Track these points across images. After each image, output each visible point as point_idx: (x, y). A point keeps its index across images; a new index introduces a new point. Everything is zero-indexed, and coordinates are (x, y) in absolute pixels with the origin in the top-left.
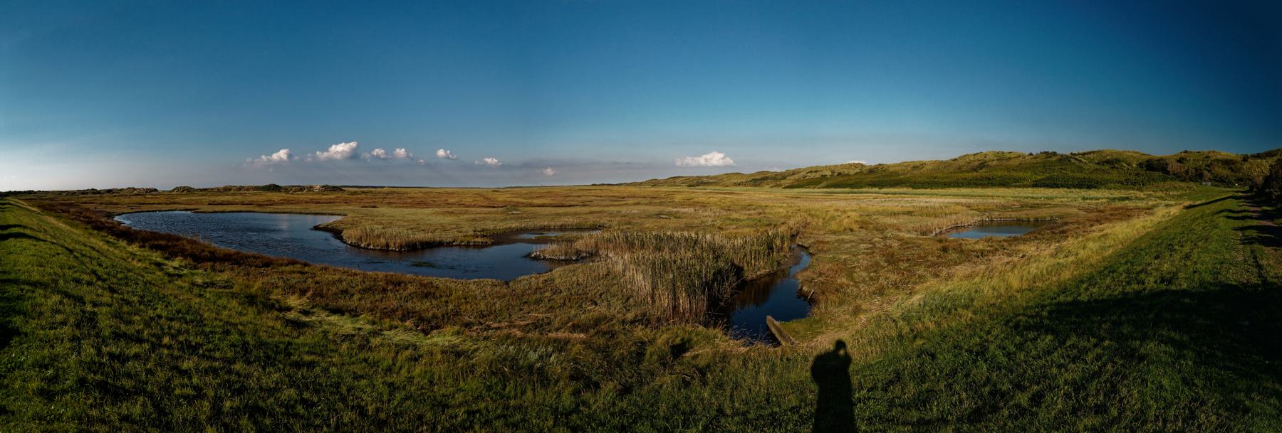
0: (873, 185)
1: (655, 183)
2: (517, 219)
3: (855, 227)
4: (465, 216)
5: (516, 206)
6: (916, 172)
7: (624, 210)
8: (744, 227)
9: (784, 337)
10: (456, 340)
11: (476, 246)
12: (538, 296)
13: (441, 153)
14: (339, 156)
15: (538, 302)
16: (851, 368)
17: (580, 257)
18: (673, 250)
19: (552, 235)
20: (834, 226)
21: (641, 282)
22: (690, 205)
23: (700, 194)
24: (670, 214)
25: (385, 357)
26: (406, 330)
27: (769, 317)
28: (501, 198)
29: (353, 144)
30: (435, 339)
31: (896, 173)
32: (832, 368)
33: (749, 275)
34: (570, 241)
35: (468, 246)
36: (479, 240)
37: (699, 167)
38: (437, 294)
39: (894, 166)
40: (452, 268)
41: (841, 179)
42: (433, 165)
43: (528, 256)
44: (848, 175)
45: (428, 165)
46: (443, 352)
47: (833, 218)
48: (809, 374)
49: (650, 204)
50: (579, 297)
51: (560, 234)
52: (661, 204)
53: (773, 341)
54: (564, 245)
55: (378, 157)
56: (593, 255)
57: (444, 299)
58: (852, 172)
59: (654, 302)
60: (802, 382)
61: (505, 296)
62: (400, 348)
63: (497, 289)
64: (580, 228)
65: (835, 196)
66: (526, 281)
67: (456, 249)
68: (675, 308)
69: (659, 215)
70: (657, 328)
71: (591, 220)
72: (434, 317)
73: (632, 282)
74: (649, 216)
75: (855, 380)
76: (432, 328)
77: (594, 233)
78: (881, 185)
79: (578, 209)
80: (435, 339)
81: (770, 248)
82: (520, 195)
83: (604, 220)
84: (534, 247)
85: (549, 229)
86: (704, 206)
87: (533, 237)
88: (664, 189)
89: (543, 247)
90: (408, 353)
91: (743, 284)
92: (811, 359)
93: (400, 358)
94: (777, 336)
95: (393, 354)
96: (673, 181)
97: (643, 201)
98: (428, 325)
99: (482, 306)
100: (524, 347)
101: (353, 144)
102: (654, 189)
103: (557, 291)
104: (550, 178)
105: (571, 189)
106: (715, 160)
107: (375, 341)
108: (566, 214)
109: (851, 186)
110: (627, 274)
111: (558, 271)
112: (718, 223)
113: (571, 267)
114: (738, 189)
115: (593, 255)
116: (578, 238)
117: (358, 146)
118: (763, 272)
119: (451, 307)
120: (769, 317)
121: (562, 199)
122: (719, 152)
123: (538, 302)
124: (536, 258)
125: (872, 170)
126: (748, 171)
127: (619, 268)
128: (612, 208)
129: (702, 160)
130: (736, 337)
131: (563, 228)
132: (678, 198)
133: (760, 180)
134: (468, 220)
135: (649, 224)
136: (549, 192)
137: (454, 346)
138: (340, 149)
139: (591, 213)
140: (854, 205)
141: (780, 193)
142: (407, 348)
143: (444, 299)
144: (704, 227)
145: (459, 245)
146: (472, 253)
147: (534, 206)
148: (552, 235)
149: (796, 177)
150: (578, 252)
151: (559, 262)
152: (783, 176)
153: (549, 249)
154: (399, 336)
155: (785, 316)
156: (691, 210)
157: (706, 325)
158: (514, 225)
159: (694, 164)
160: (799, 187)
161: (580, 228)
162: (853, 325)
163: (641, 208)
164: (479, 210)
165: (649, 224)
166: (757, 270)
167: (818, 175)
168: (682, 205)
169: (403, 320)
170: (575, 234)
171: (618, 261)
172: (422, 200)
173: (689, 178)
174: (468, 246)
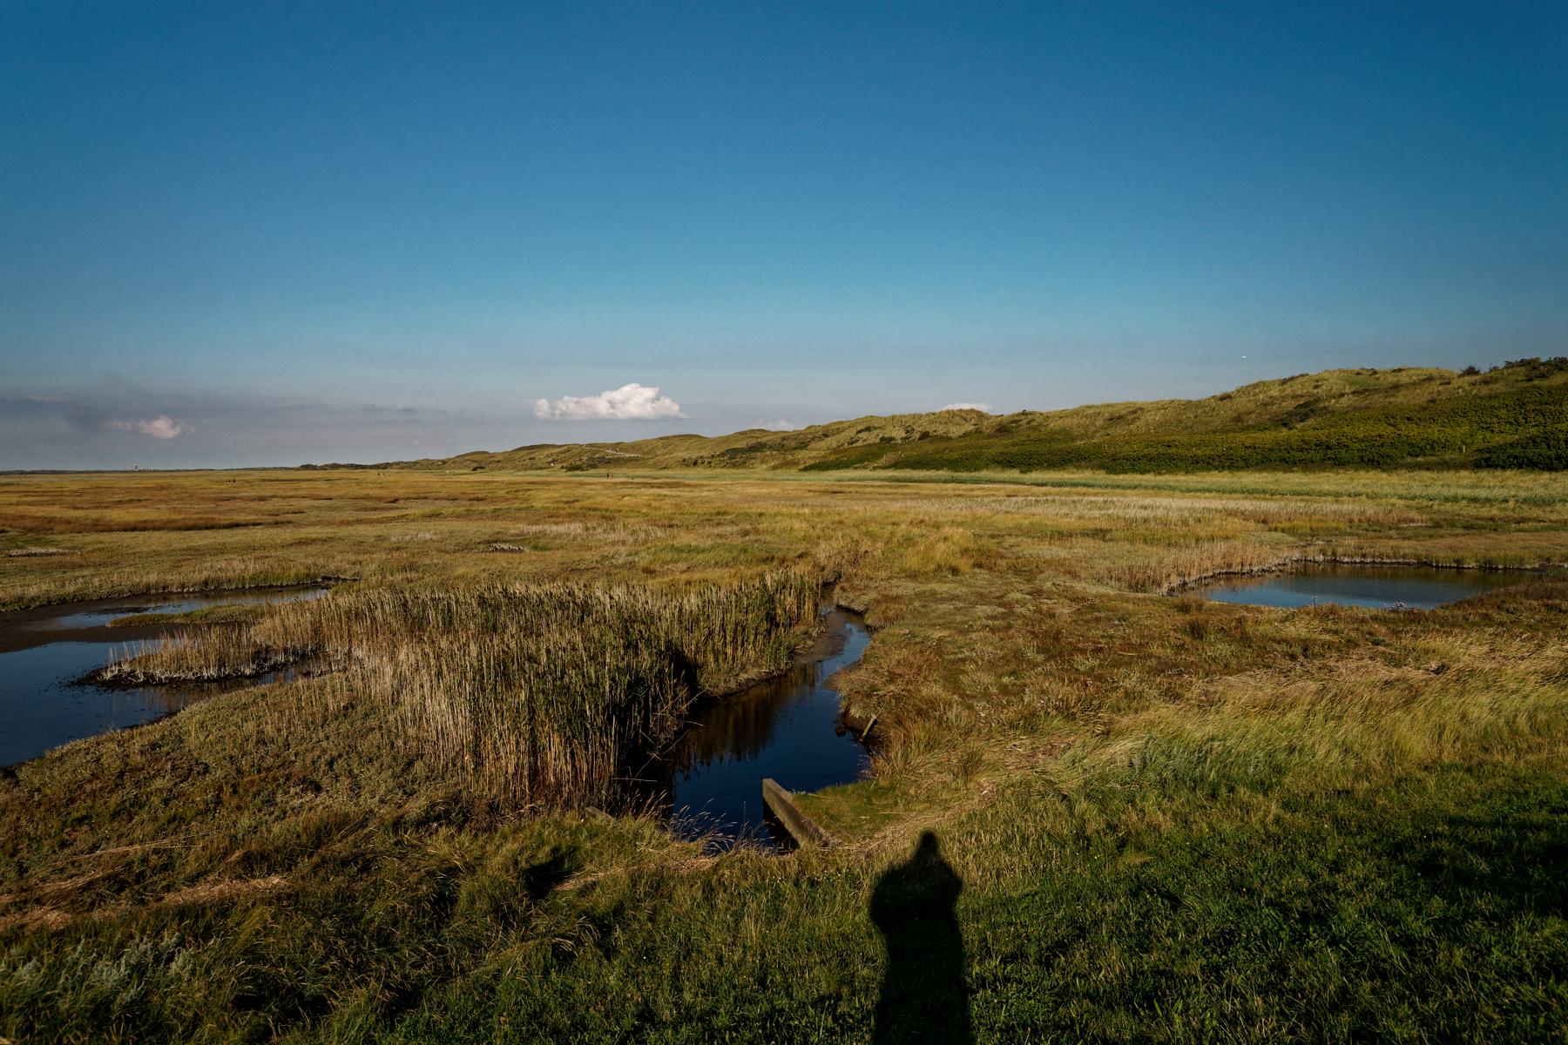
0: (1006, 462)
1: (480, 462)
2: (46, 570)
3: (964, 564)
5: (44, 528)
6: (1118, 431)
7: (396, 533)
8: (706, 566)
9: (802, 827)
12: (129, 792)
15: (124, 812)
16: (962, 903)
17: (266, 666)
18: (529, 631)
19: (173, 610)
20: (912, 561)
21: (444, 714)
22: (572, 517)
23: (598, 488)
24: (522, 539)
27: (768, 783)
31: (1067, 435)
32: (918, 898)
33: (716, 680)
34: (233, 624)
37: (595, 421)
39: (1061, 416)
41: (928, 448)
43: (91, 679)
44: (945, 438)
47: (909, 541)
48: (863, 916)
49: (467, 515)
50: (264, 777)
51: (201, 607)
52: (496, 515)
53: (781, 839)
54: (214, 637)
56: (306, 657)
58: (955, 431)
59: (479, 764)
60: (845, 938)
64: (264, 587)
65: (913, 488)
68: (535, 774)
69: (491, 544)
70: (491, 829)
71: (300, 562)
73: (419, 717)
74: (466, 547)
75: (971, 932)
77: (310, 598)
78: (1024, 461)
79: (259, 534)
81: (771, 619)
82: (57, 497)
83: (339, 562)
84: (112, 651)
85: (163, 594)
86: (608, 517)
87: (107, 620)
88: (505, 476)
89: (143, 647)
91: (704, 705)
92: (866, 882)
94: (789, 826)
96: (528, 456)
97: (448, 508)
100: (75, 953)
102: (479, 477)
103: (195, 769)
104: (163, 446)
105: (236, 478)
106: (632, 404)
108: (221, 550)
109: (953, 465)
110: (406, 698)
111: (193, 712)
112: (644, 559)
113: (241, 696)
114: (692, 474)
115: (306, 657)
116: (257, 615)
118: (752, 673)
120: (768, 783)
121: (211, 509)
122: (644, 385)
123: (124, 812)
124: (122, 683)
125: (1005, 428)
126: (718, 429)
127: (387, 682)
128: (362, 530)
130: (687, 834)
131: (209, 590)
132: (541, 499)
133: (745, 451)
135: (466, 567)
136: (163, 487)
139: (302, 543)
140: (958, 509)
141: (795, 482)
144: (608, 571)
147: (109, 528)
148: (173, 610)
149: (832, 442)
150: (261, 654)
151: (200, 686)
152: (801, 441)
153: (162, 654)
155: (808, 779)
156: (576, 528)
157: (615, 809)
158: (36, 588)
159: (583, 413)
160: (838, 465)
161: (264, 587)
162: (963, 796)
163: (444, 526)
165: (466, 567)
166: (735, 669)
167: (873, 438)
168: (553, 516)
170: (249, 603)
171: (379, 668)
173: (569, 449)
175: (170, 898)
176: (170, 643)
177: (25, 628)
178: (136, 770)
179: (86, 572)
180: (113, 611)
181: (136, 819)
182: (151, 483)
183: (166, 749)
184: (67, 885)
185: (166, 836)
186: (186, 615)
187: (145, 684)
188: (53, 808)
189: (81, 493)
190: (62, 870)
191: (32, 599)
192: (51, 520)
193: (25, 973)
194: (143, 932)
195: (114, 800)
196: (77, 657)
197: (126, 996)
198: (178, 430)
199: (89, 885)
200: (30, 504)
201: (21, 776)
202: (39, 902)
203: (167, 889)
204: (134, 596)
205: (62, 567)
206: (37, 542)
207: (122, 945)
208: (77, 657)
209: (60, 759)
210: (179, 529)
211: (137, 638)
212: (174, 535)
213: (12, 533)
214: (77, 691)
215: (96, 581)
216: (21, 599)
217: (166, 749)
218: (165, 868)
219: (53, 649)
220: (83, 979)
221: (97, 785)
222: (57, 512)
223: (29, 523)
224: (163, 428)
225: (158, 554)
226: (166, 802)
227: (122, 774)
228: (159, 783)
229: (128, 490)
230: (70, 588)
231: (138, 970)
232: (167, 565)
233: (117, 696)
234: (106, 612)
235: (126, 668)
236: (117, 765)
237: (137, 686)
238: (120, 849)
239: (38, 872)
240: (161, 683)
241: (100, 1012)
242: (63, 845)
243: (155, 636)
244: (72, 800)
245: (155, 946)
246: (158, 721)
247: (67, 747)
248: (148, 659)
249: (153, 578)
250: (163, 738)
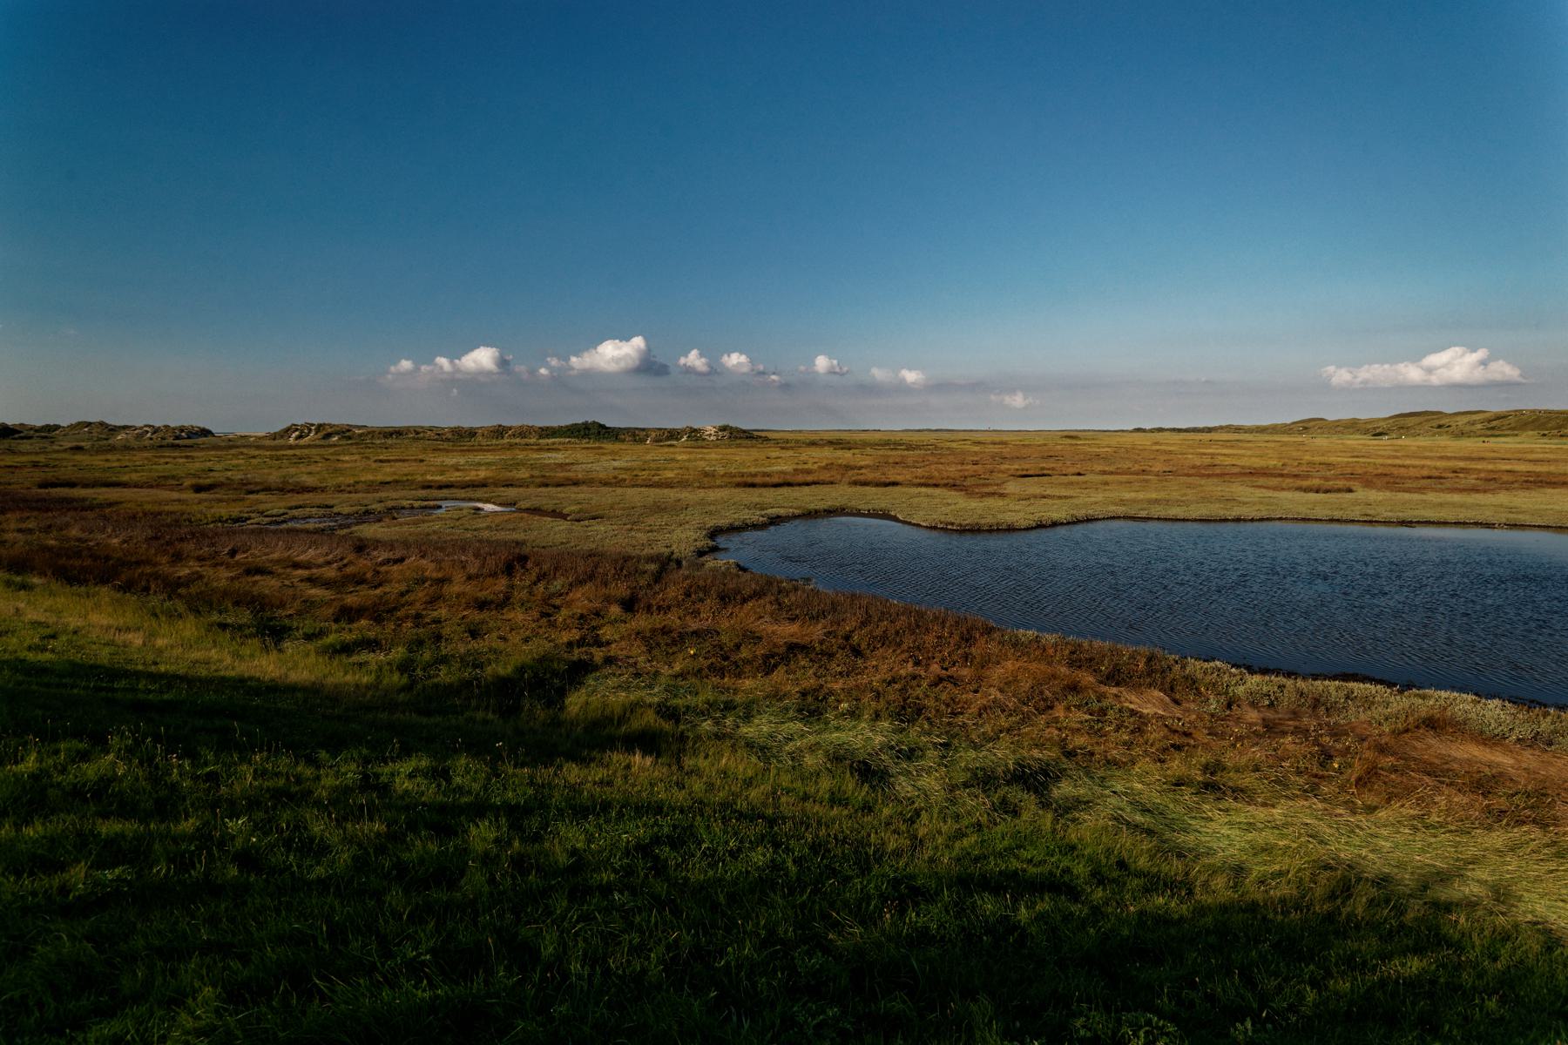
14: (613, 367)
45: (786, 387)
55: (689, 370)
101: (638, 342)
106: (1454, 367)
117: (649, 349)
129: (1413, 373)
138: (615, 353)
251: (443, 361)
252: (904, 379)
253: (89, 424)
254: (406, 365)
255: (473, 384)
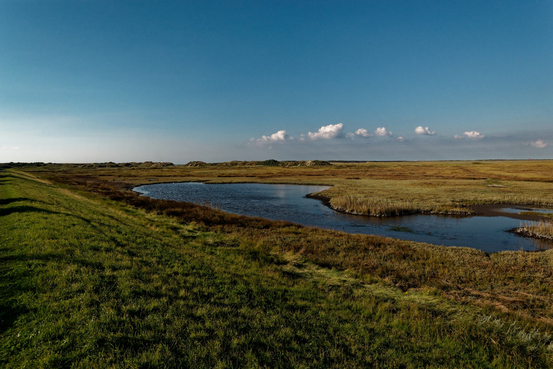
4: (443, 188)
5: (497, 179)
10: (433, 300)
11: (454, 215)
12: (526, 274)
13: (419, 130)
14: (327, 136)
25: (366, 306)
26: (385, 285)
28: (483, 170)
29: (339, 126)
30: (412, 296)
35: (446, 215)
36: (458, 209)
38: (415, 256)
40: (429, 234)
42: (411, 141)
43: (513, 231)
46: (420, 309)
55: (361, 136)
57: (421, 261)
61: (485, 267)
62: (379, 300)
63: (478, 258)
66: (506, 257)
67: (434, 218)
72: (412, 276)
76: (410, 286)
80: (412, 296)
82: (502, 168)
85: (540, 205)
87: (519, 212)
89: (532, 224)
90: (387, 305)
93: (379, 308)
95: (373, 305)
98: (406, 283)
99: (461, 272)
101: (339, 126)
107: (358, 292)
117: (343, 127)
119: (428, 269)
123: (527, 281)
134: (445, 191)
137: (431, 305)
142: (386, 301)
143: (421, 261)
145: (437, 214)
146: (451, 222)
147: (520, 180)
154: (379, 290)
158: (496, 198)
164: (458, 181)
169: (382, 276)
172: (401, 172)
174: (446, 215)
175: (543, 319)
176: (543, 224)
177: (492, 210)
178: (529, 267)
179: (512, 194)
180: (521, 209)
181: (530, 285)
182: (535, 164)
183: (540, 263)
184: (507, 298)
185: (542, 295)
186: (549, 215)
187: (532, 237)
188: (501, 270)
189: (510, 167)
190: (505, 293)
191: (494, 201)
192: (501, 176)
193: (497, 321)
194: (537, 328)
195: (522, 275)
196: (511, 223)
197: (532, 348)
198: (545, 145)
199: (514, 302)
200: (494, 170)
201: (491, 257)
202: (498, 300)
203: (542, 315)
204: (528, 204)
205: (504, 191)
206: (496, 183)
207: (529, 329)
208: (511, 223)
209: (503, 255)
210: (546, 182)
211: (530, 220)
212: (544, 184)
213: (489, 179)
214: (508, 234)
215: (515, 198)
216: (491, 200)
217: (540, 263)
218: (542, 307)
219: (500, 218)
220: (516, 334)
221: (516, 268)
222: (502, 173)
223: (494, 177)
224: (540, 144)
225: (537, 190)
226: (541, 283)
227: (524, 267)
228: (538, 274)
229: (526, 167)
230: (506, 199)
231: (535, 341)
232: (541, 195)
233: (521, 239)
234: (518, 209)
235: (525, 229)
236: (522, 264)
237: (529, 237)
238: (524, 293)
239: (497, 290)
240: (538, 238)
241: (522, 348)
242: (505, 284)
243: (537, 220)
244: (507, 270)
245: (541, 336)
246: (538, 251)
247: (505, 252)
248: (534, 228)
249: (536, 199)
250: (540, 258)
251: (264, 137)
252: (467, 136)
253: (148, 162)
254: (252, 139)
255: (277, 144)
